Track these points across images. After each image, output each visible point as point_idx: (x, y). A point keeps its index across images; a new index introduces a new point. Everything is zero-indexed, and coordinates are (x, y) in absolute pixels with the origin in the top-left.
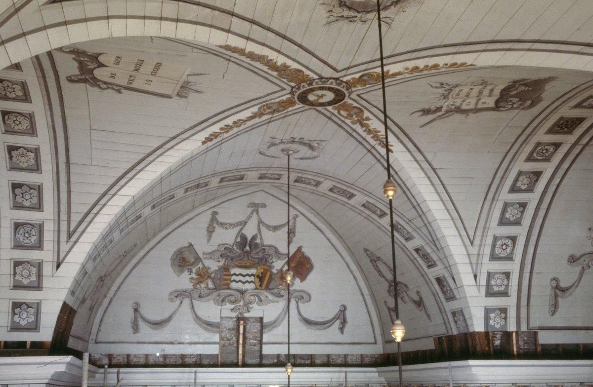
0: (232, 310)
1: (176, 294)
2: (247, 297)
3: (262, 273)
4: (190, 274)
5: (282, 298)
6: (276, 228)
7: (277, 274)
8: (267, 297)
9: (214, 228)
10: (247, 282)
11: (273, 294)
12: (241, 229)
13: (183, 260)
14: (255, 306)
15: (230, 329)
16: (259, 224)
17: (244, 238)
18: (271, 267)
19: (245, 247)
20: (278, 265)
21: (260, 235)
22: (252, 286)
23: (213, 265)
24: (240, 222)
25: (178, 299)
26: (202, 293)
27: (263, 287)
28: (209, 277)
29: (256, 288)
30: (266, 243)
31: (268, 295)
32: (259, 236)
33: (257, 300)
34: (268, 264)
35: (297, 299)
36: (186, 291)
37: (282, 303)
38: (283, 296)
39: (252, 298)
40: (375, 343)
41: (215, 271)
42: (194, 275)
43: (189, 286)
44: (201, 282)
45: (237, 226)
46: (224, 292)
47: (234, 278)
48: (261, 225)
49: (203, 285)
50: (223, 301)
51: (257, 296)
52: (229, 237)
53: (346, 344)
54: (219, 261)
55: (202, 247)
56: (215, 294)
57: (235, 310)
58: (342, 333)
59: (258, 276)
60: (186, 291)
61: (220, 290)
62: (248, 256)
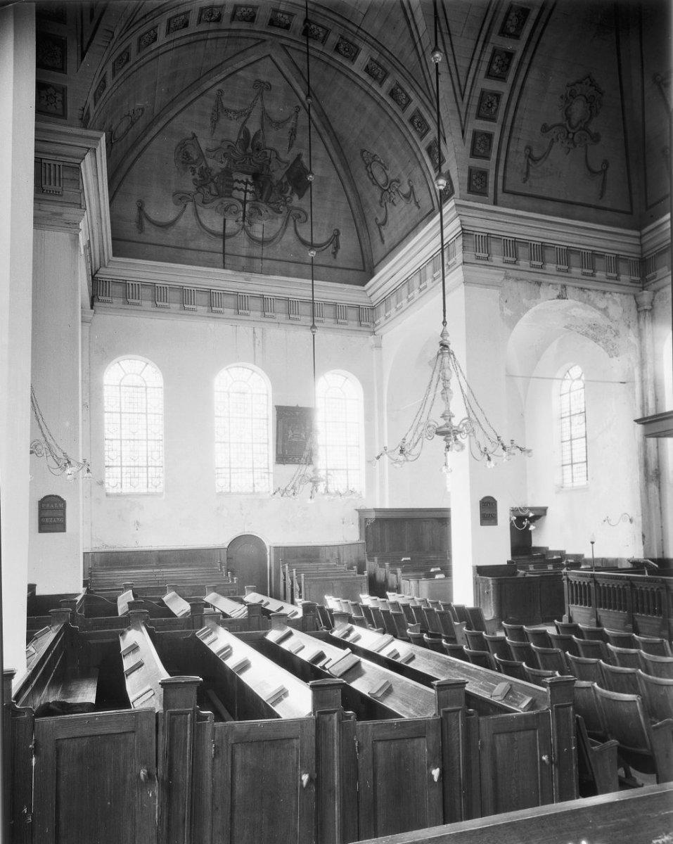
12: (245, 122)
13: (186, 155)
17: (247, 133)
19: (247, 147)
38: (281, 212)
41: (218, 175)
42: (197, 176)
46: (227, 201)
47: (236, 185)
56: (217, 202)
58: (335, 258)
62: (250, 159)
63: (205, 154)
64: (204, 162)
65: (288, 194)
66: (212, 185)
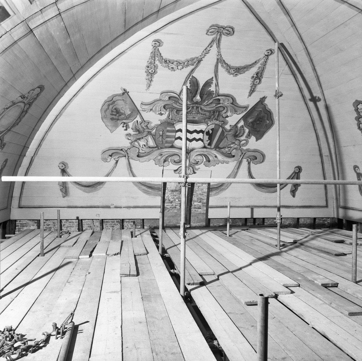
0: (175, 171)
1: (110, 152)
2: (194, 156)
3: (212, 130)
4: (126, 130)
5: (233, 159)
6: (239, 70)
7: (230, 130)
8: (216, 157)
9: (156, 67)
10: (194, 139)
11: (223, 154)
12: (193, 71)
14: (202, 166)
15: (172, 191)
16: (217, 63)
17: (195, 83)
18: (225, 123)
20: (233, 119)
21: (217, 80)
22: (200, 144)
23: (154, 119)
24: (192, 59)
25: (113, 159)
26: (141, 151)
27: (213, 146)
28: (150, 133)
29: (205, 147)
30: (221, 92)
31: (217, 155)
32: (214, 81)
33: (205, 160)
34: (221, 119)
35: (249, 160)
36: (121, 150)
37: (232, 164)
38: (234, 156)
39: (200, 158)
40: (327, 206)
41: (157, 126)
42: (130, 131)
43: (125, 143)
44: (139, 139)
45: (187, 66)
46: (167, 151)
48: (220, 65)
49: (142, 142)
50: (165, 161)
51: (205, 156)
52: (173, 81)
53: (297, 207)
54: (161, 114)
55: (141, 95)
56: (156, 153)
57: (178, 171)
58: (294, 196)
59: (208, 133)
60: (121, 150)
61: (161, 148)
62: (197, 107)
63: (139, 108)
64: (138, 116)
65: (243, 138)
66: (150, 139)
